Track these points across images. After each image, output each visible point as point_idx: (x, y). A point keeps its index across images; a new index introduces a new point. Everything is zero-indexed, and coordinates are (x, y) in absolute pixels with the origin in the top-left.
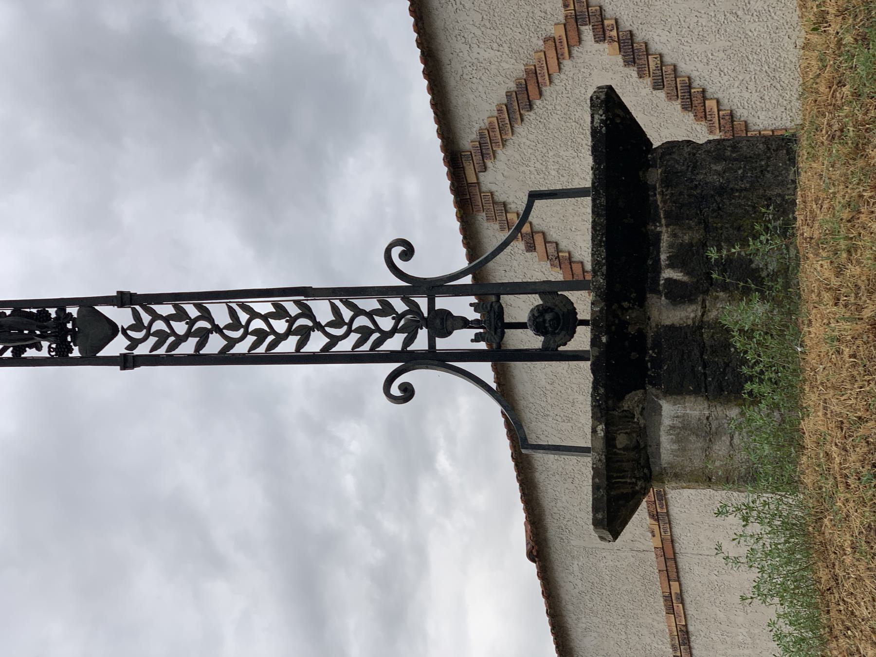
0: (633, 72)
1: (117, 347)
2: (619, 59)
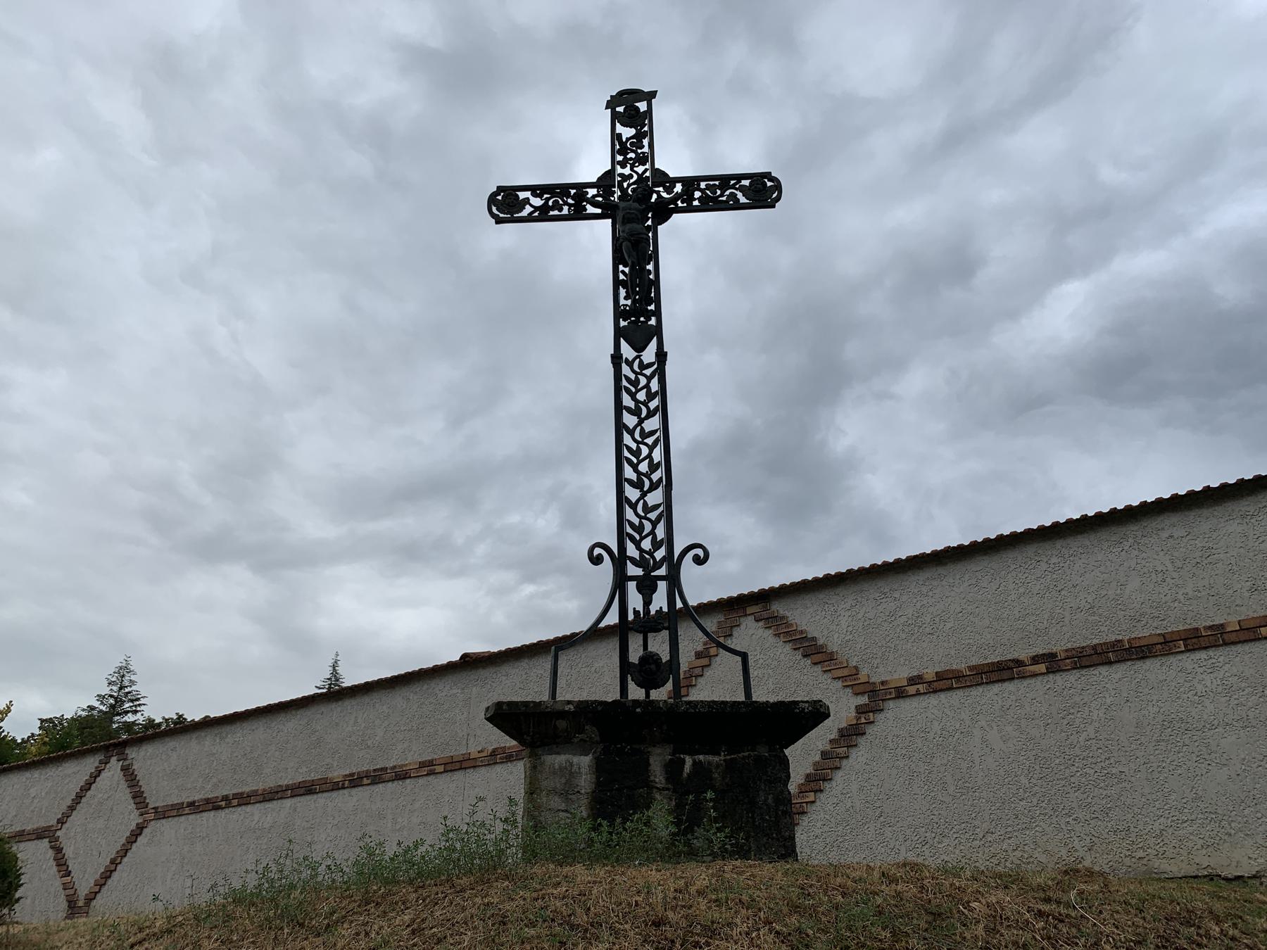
1: (627, 351)
2: (844, 725)
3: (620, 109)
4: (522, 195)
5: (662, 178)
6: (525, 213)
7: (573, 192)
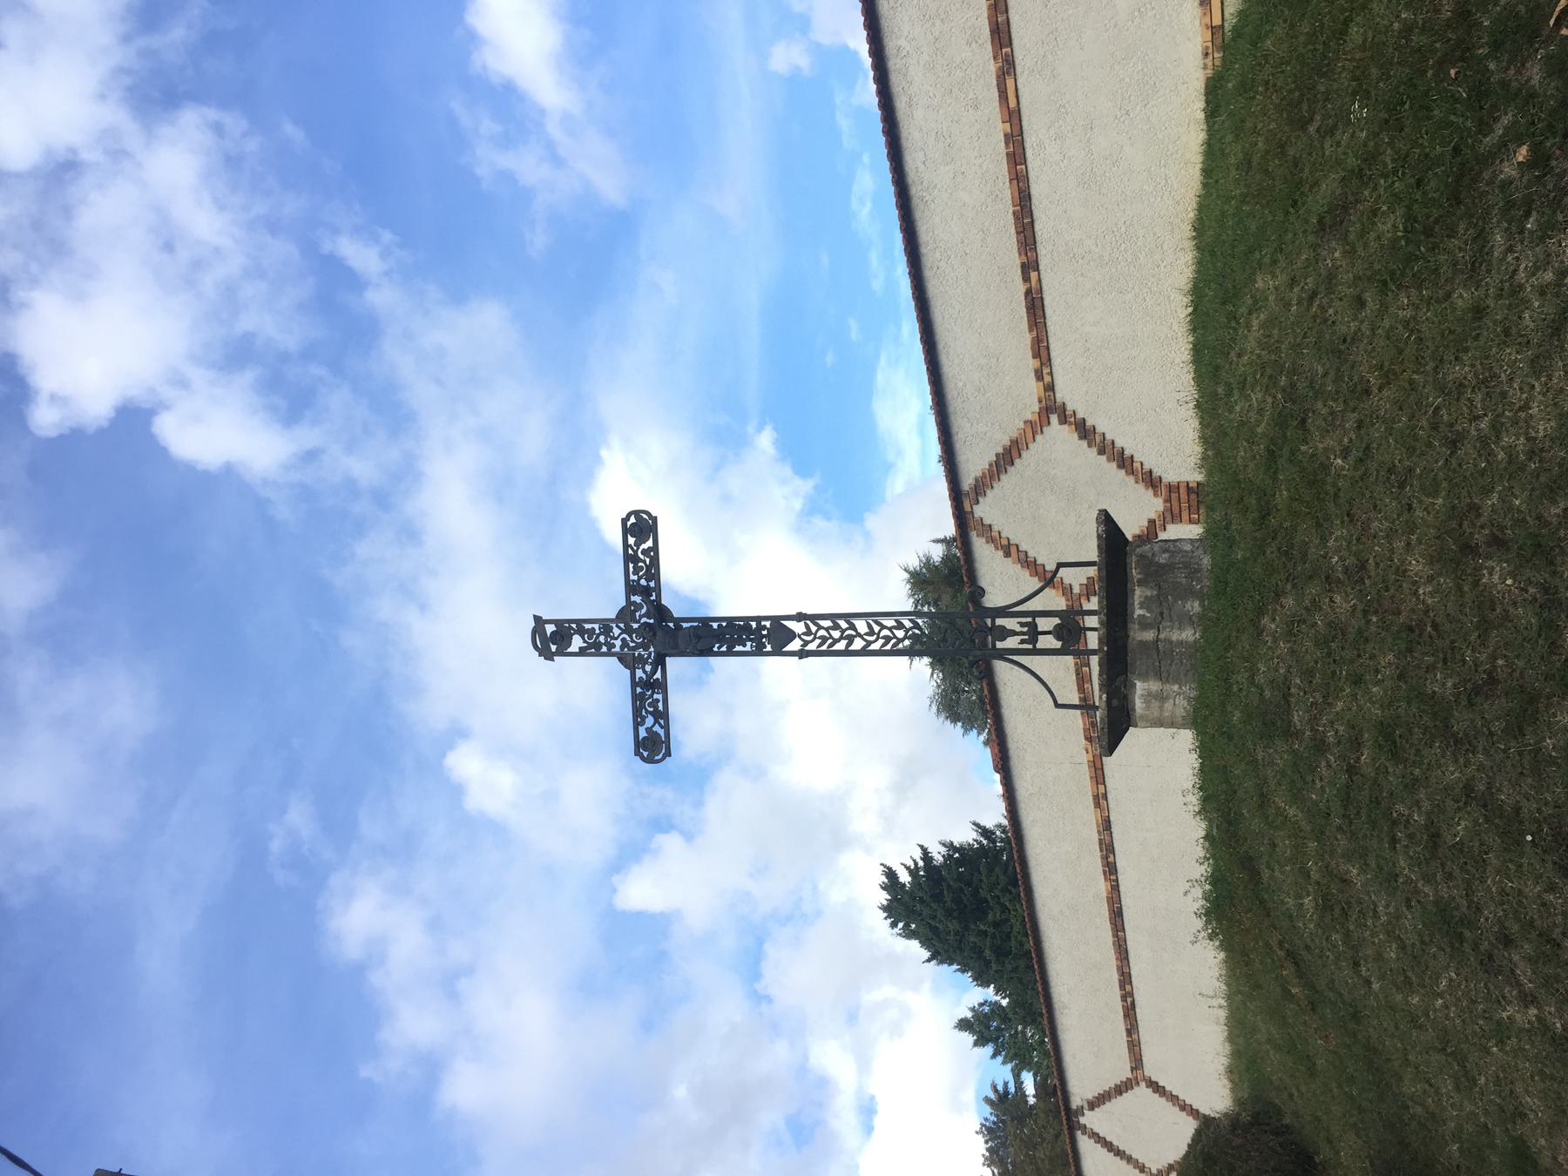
0: (1085, 443)
1: (795, 645)
2: (1076, 435)
3: (554, 648)
4: (643, 733)
5: (626, 615)
6: (661, 732)
7: (639, 690)
